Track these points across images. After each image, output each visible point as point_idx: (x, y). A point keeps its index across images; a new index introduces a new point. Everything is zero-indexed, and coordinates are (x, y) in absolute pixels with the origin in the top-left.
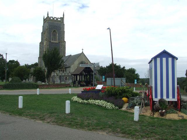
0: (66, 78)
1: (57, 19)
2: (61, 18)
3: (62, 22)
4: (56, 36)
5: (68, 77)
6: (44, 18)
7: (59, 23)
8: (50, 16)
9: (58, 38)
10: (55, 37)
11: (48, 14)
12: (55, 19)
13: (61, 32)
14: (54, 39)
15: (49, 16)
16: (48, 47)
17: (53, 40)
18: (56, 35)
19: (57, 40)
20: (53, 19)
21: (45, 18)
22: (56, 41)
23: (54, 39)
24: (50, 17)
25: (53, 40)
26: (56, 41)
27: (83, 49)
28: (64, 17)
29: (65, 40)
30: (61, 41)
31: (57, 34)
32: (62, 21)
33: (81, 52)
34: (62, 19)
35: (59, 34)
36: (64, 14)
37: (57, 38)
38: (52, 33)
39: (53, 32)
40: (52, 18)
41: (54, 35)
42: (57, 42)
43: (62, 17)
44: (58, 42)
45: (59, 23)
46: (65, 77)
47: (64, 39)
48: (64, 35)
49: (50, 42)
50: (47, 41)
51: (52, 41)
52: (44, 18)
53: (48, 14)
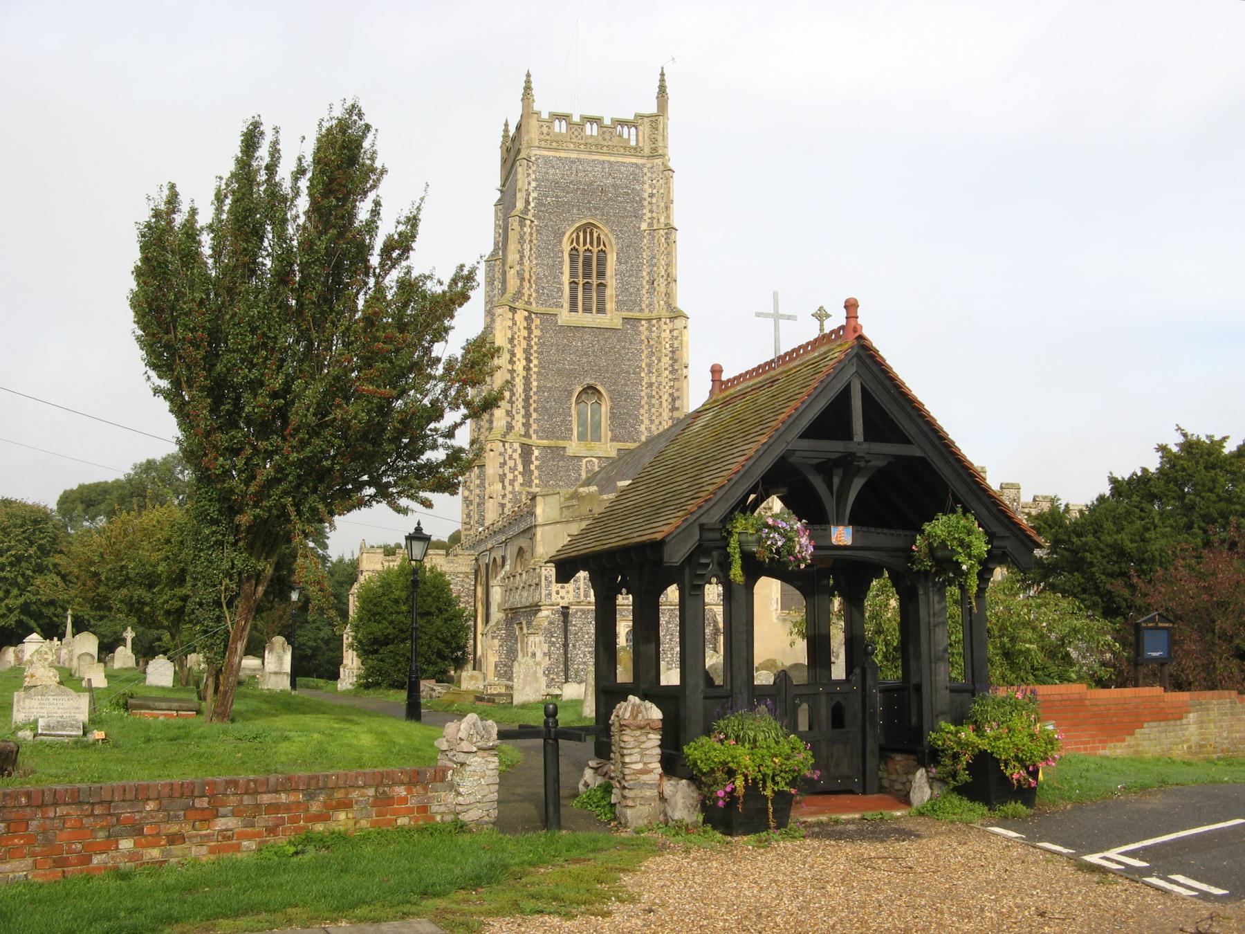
3: (655, 149)
4: (601, 274)
6: (506, 130)
8: (544, 105)
9: (623, 288)
11: (528, 88)
12: (591, 130)
13: (638, 233)
14: (587, 299)
15: (536, 107)
16: (527, 369)
17: (573, 307)
18: (602, 262)
19: (610, 306)
20: (576, 127)
21: (512, 131)
22: (601, 310)
23: (587, 299)
24: (545, 116)
26: (601, 310)
29: (681, 304)
30: (646, 314)
31: (612, 260)
32: (654, 141)
34: (655, 121)
35: (630, 251)
36: (662, 89)
37: (610, 292)
38: (566, 247)
40: (560, 127)
42: (611, 318)
43: (653, 109)
44: (618, 323)
45: (627, 160)
49: (548, 319)
50: (520, 316)
51: (565, 317)
52: (506, 130)
53: (528, 88)
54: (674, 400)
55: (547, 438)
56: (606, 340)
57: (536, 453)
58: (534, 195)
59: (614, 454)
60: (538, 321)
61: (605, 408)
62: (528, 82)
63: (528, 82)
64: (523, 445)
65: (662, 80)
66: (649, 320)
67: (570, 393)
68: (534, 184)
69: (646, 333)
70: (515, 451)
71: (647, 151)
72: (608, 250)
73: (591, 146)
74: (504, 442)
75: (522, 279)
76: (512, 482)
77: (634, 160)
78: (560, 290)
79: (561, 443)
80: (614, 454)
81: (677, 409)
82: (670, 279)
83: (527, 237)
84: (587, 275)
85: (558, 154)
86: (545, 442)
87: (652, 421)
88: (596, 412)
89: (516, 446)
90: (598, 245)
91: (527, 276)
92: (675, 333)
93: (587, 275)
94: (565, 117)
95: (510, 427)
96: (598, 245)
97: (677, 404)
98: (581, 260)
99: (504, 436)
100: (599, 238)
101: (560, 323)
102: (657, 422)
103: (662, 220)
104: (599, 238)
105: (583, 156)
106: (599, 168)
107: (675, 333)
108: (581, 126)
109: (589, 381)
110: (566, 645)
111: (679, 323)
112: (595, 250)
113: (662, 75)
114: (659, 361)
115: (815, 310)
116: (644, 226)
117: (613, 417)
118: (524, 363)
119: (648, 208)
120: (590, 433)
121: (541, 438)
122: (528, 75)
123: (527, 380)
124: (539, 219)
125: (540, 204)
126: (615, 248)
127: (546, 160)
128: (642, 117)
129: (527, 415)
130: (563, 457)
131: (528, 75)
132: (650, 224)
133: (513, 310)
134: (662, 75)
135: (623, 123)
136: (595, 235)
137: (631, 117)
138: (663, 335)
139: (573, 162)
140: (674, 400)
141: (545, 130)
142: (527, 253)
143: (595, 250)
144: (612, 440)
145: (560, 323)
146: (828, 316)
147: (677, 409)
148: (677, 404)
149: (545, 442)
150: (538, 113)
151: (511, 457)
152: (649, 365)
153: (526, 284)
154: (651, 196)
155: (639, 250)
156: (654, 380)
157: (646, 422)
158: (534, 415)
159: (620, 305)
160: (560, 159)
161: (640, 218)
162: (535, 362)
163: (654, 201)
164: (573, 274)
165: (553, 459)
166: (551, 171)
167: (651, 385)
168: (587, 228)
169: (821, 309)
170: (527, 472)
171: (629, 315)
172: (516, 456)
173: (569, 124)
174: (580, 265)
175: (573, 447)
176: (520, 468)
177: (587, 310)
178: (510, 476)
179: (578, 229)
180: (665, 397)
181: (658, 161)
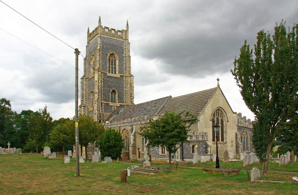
0: (193, 147)
1: (116, 32)
2: (122, 32)
3: (126, 38)
4: (115, 65)
5: (196, 146)
7: (121, 40)
8: (103, 25)
9: (120, 68)
10: (114, 67)
11: (100, 20)
13: (123, 57)
14: (112, 70)
15: (102, 25)
16: (101, 85)
17: (109, 72)
18: (115, 63)
19: (117, 72)
22: (115, 73)
23: (112, 70)
24: (103, 27)
25: (109, 72)
27: (218, 80)
28: (129, 31)
29: (132, 73)
31: (117, 62)
32: (126, 36)
33: (216, 86)
34: (125, 32)
36: (127, 24)
37: (117, 69)
39: (110, 57)
40: (107, 30)
41: (113, 63)
42: (118, 75)
43: (125, 29)
44: (119, 76)
45: (121, 40)
46: (191, 146)
47: (130, 71)
48: (130, 64)
50: (100, 73)
51: (108, 74)
53: (100, 20)
54: (131, 94)
55: (105, 101)
56: (117, 80)
57: (103, 104)
58: (101, 45)
59: (119, 106)
60: (103, 74)
61: (117, 95)
62: (100, 18)
63: (100, 18)
64: (101, 102)
65: (127, 23)
66: (125, 76)
67: (110, 91)
68: (101, 43)
69: (125, 79)
70: (100, 104)
71: (124, 38)
72: (116, 59)
73: (113, 36)
74: (98, 102)
75: (100, 64)
76: (99, 111)
77: (122, 40)
78: (107, 68)
79: (108, 103)
80: (119, 106)
81: (132, 96)
82: (130, 67)
83: (100, 55)
84: (112, 65)
85: (106, 36)
86: (105, 102)
87: (126, 99)
88: (115, 96)
89: (100, 103)
90: (114, 58)
91: (100, 64)
92: (131, 80)
93: (112, 65)
94: (108, 28)
95: (98, 98)
96: (114, 58)
97: (132, 95)
98: (111, 61)
99: (98, 100)
100: (114, 57)
101: (107, 75)
102: (127, 99)
103: (128, 54)
104: (114, 57)
105: (111, 38)
106: (115, 41)
107: (131, 80)
108: (111, 31)
109: (113, 89)
110: (182, 150)
111: (132, 77)
112: (114, 59)
113: (127, 21)
114: (128, 86)
115: (217, 79)
116: (124, 55)
117: (119, 97)
118: (101, 84)
119: (125, 51)
120: (114, 101)
121: (104, 101)
122: (100, 17)
123: (101, 87)
124: (102, 51)
125: (103, 47)
126: (118, 59)
127: (104, 37)
128: (123, 30)
129: (101, 96)
130: (109, 106)
131: (100, 17)
132: (125, 55)
133: (99, 71)
134: (127, 21)
135: (119, 31)
136: (114, 56)
137: (121, 30)
138: (129, 80)
139: (109, 39)
140: (131, 94)
141: (104, 30)
142: (100, 58)
143: (114, 59)
144: (118, 102)
145: (107, 75)
146: (219, 80)
147: (132, 96)
148: (132, 95)
149: (105, 102)
150: (102, 26)
151: (99, 105)
152: (125, 86)
153: (100, 65)
154: (125, 48)
155: (123, 60)
156: (127, 90)
157: (125, 99)
158: (102, 96)
159: (119, 73)
160: (107, 37)
161: (123, 53)
162: (102, 84)
163: (126, 50)
164: (109, 64)
165: (107, 106)
166: (105, 40)
167: (126, 91)
168: (112, 54)
169: (218, 78)
170: (102, 109)
171: (121, 75)
172: (100, 105)
173: (109, 30)
174: (111, 62)
175: (111, 104)
176: (101, 108)
177: (112, 73)
178: (99, 109)
179: (110, 55)
180: (129, 94)
181: (127, 41)
